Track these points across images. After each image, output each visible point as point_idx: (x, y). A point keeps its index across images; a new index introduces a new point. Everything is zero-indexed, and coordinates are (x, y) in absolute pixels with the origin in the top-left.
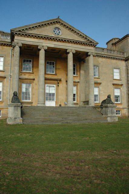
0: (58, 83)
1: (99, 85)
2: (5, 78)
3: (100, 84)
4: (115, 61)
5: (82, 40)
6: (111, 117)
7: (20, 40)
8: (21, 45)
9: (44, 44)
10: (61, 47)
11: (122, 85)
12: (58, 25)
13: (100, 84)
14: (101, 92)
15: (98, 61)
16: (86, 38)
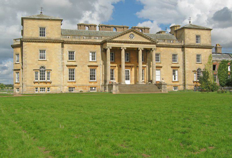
0: (132, 68)
1: (160, 69)
2: (97, 66)
3: (161, 67)
4: (173, 49)
5: (148, 41)
6: (163, 90)
7: (109, 45)
8: (111, 48)
9: (124, 46)
10: (134, 47)
11: (179, 67)
12: (132, 33)
13: (161, 67)
14: (162, 73)
15: (160, 50)
16: (150, 39)
